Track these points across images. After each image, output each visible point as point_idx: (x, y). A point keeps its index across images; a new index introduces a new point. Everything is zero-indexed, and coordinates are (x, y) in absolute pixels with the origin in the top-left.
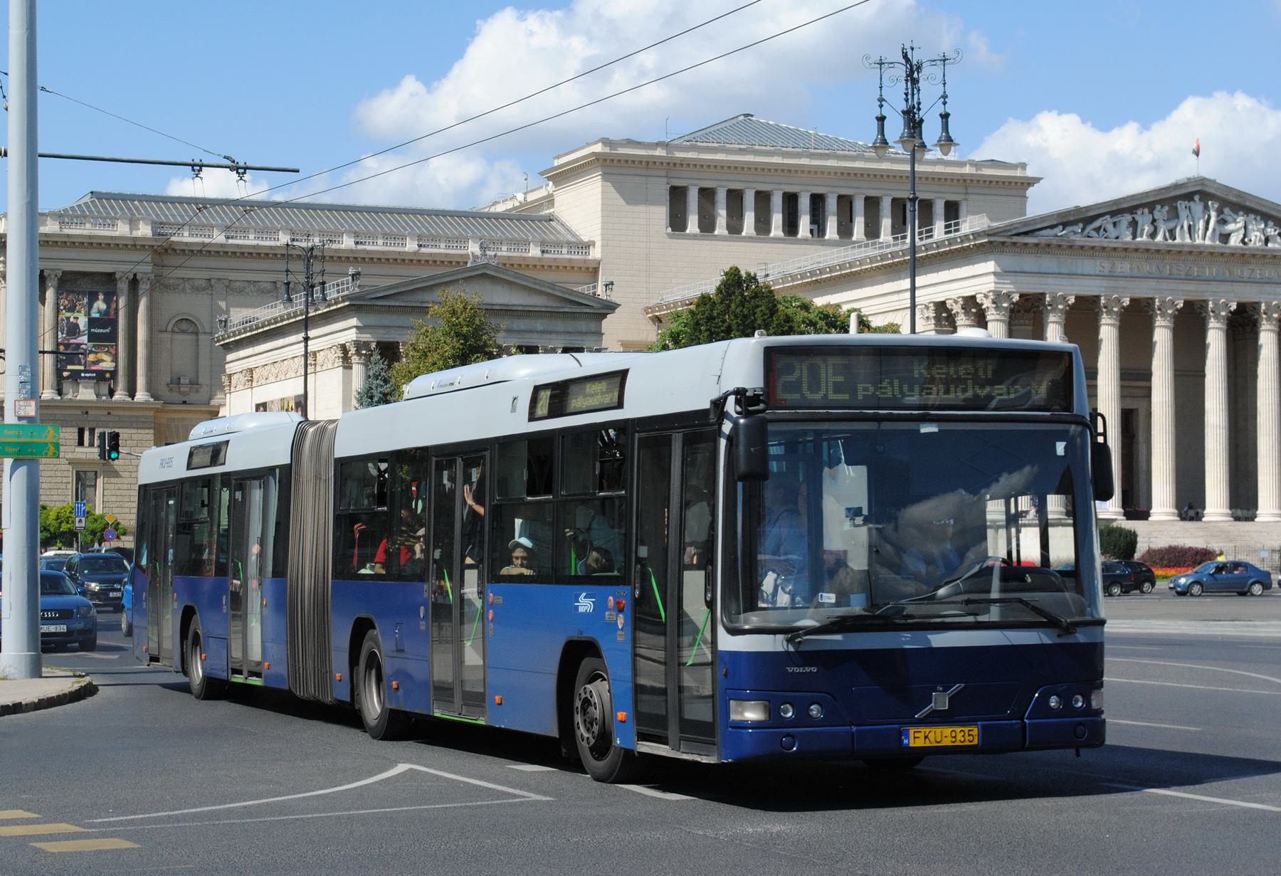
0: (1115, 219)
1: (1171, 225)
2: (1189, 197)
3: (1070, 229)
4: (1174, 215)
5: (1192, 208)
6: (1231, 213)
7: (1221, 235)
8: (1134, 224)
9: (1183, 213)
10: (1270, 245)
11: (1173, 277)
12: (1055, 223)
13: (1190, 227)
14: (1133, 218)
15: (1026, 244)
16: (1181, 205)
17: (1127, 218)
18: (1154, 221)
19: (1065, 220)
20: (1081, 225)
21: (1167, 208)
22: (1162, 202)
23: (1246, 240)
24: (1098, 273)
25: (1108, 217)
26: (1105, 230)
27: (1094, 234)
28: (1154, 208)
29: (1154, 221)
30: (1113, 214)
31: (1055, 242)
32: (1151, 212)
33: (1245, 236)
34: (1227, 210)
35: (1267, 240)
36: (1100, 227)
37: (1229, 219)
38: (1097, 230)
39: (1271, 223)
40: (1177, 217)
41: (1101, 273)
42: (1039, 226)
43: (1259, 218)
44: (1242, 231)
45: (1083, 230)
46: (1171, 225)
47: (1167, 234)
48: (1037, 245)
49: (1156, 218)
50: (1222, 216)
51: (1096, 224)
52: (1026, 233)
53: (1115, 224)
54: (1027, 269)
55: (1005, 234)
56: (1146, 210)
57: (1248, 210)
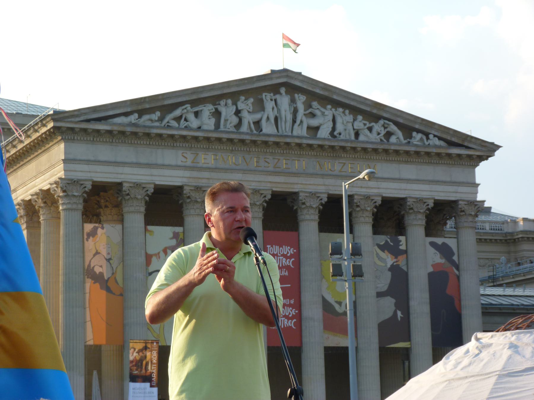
0: (196, 109)
1: (257, 116)
2: (275, 89)
3: (146, 117)
4: (260, 106)
5: (279, 101)
6: (319, 107)
7: (309, 128)
8: (217, 114)
9: (269, 105)
10: (362, 138)
11: (260, 169)
12: (129, 110)
13: (276, 119)
14: (216, 109)
15: (98, 131)
16: (267, 97)
17: (207, 110)
18: (238, 112)
19: (140, 107)
20: (158, 114)
21: (252, 100)
22: (247, 93)
23: (335, 133)
24: (179, 163)
25: (188, 106)
26: (186, 120)
27: (174, 124)
28: (239, 100)
29: (238, 112)
30: (194, 103)
31: (129, 129)
32: (235, 103)
33: (334, 129)
34: (315, 104)
35: (357, 135)
36: (181, 117)
37: (318, 112)
38: (178, 119)
39: (360, 118)
40: (263, 109)
41: (183, 164)
42: (111, 113)
43: (347, 112)
44: (331, 124)
45: (161, 119)
46: (257, 116)
47: (252, 126)
48: (110, 132)
49: (239, 108)
50: (310, 110)
51: (178, 112)
52: (99, 120)
53: (197, 114)
54: (102, 158)
55: (73, 119)
56: (230, 102)
57: (337, 104)
